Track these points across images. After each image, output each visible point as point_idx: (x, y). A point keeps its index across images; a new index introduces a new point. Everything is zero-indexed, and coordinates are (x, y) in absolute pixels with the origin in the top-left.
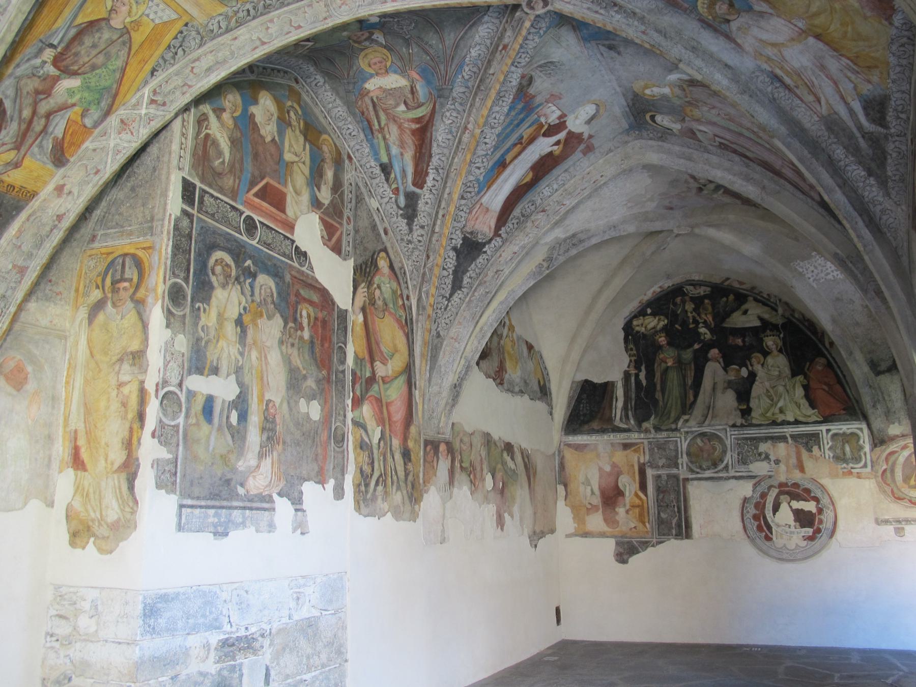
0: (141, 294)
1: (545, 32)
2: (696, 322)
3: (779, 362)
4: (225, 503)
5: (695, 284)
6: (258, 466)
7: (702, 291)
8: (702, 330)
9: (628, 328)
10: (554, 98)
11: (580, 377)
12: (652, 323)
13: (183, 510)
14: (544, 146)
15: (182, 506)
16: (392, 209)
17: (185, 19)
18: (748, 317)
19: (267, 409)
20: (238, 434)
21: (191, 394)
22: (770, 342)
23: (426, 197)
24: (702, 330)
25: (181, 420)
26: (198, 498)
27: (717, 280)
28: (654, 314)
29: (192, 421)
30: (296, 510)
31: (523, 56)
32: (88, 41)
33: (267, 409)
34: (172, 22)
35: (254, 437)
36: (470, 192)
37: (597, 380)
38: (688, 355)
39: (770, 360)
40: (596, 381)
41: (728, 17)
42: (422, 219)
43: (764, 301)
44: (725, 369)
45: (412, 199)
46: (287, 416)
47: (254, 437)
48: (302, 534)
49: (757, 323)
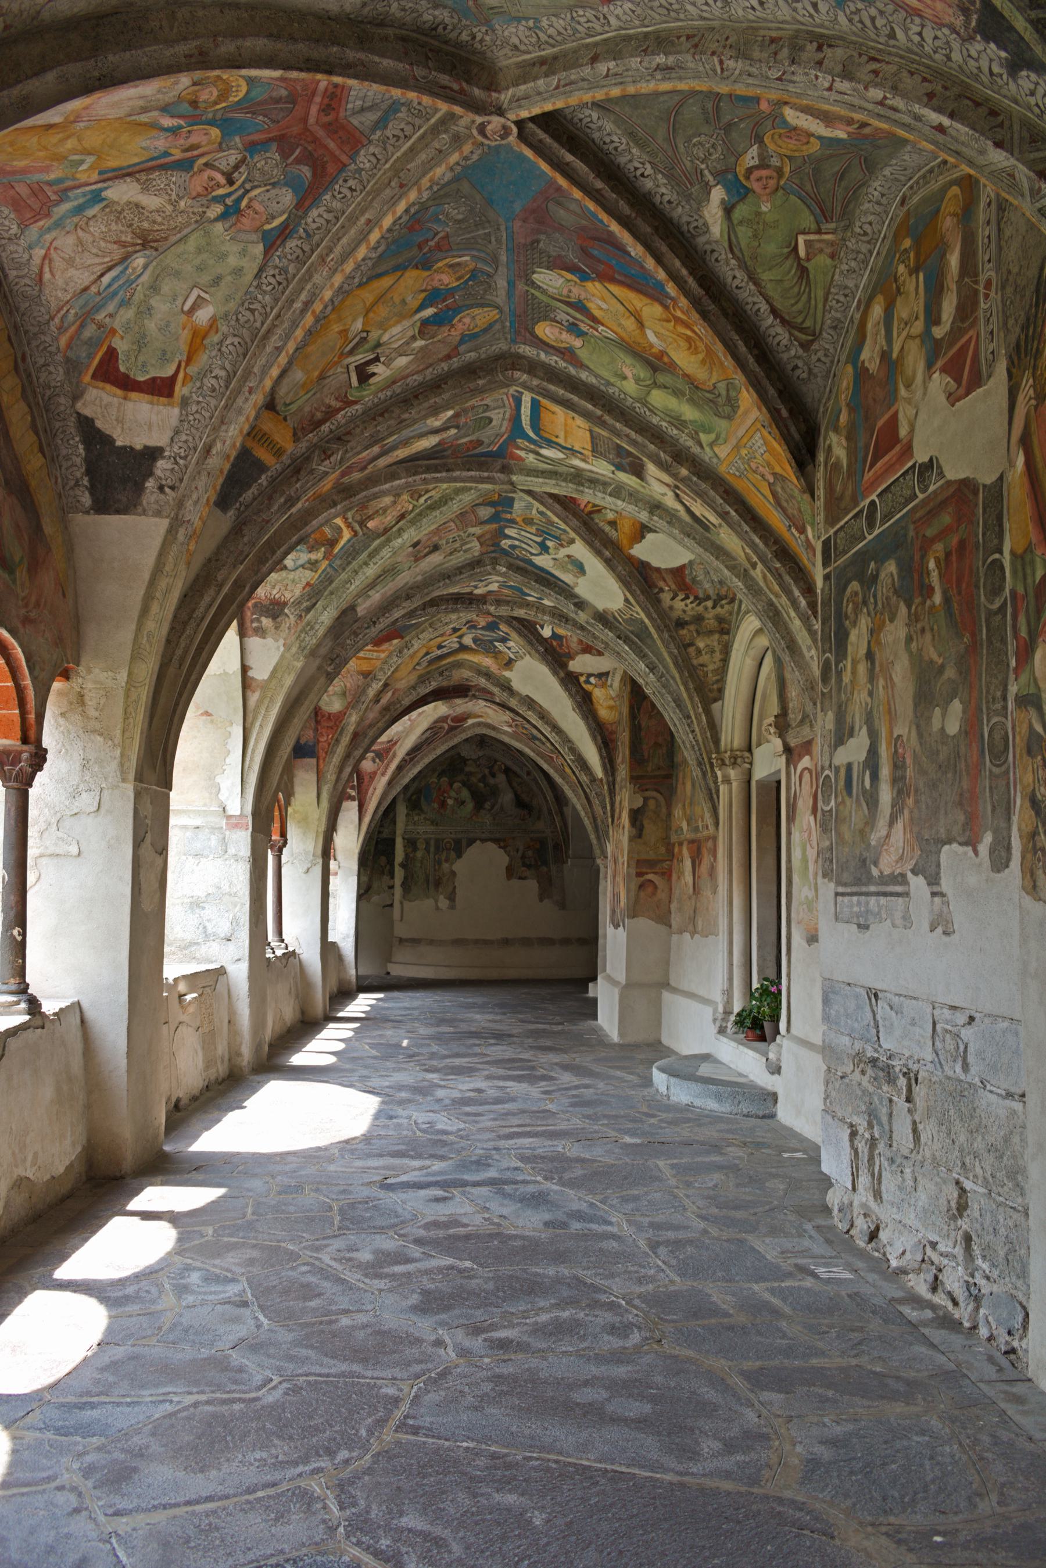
1: (527, 19)
4: (864, 889)
6: (888, 836)
13: (840, 899)
15: (837, 894)
17: (759, 426)
19: (896, 751)
20: (872, 800)
21: (837, 770)
25: (833, 803)
26: (845, 885)
29: (840, 799)
30: (934, 894)
31: (582, 20)
32: (785, 504)
33: (896, 751)
34: (763, 438)
35: (886, 795)
36: (873, 19)
41: (196, 88)
46: (918, 748)
47: (886, 795)
48: (945, 933)
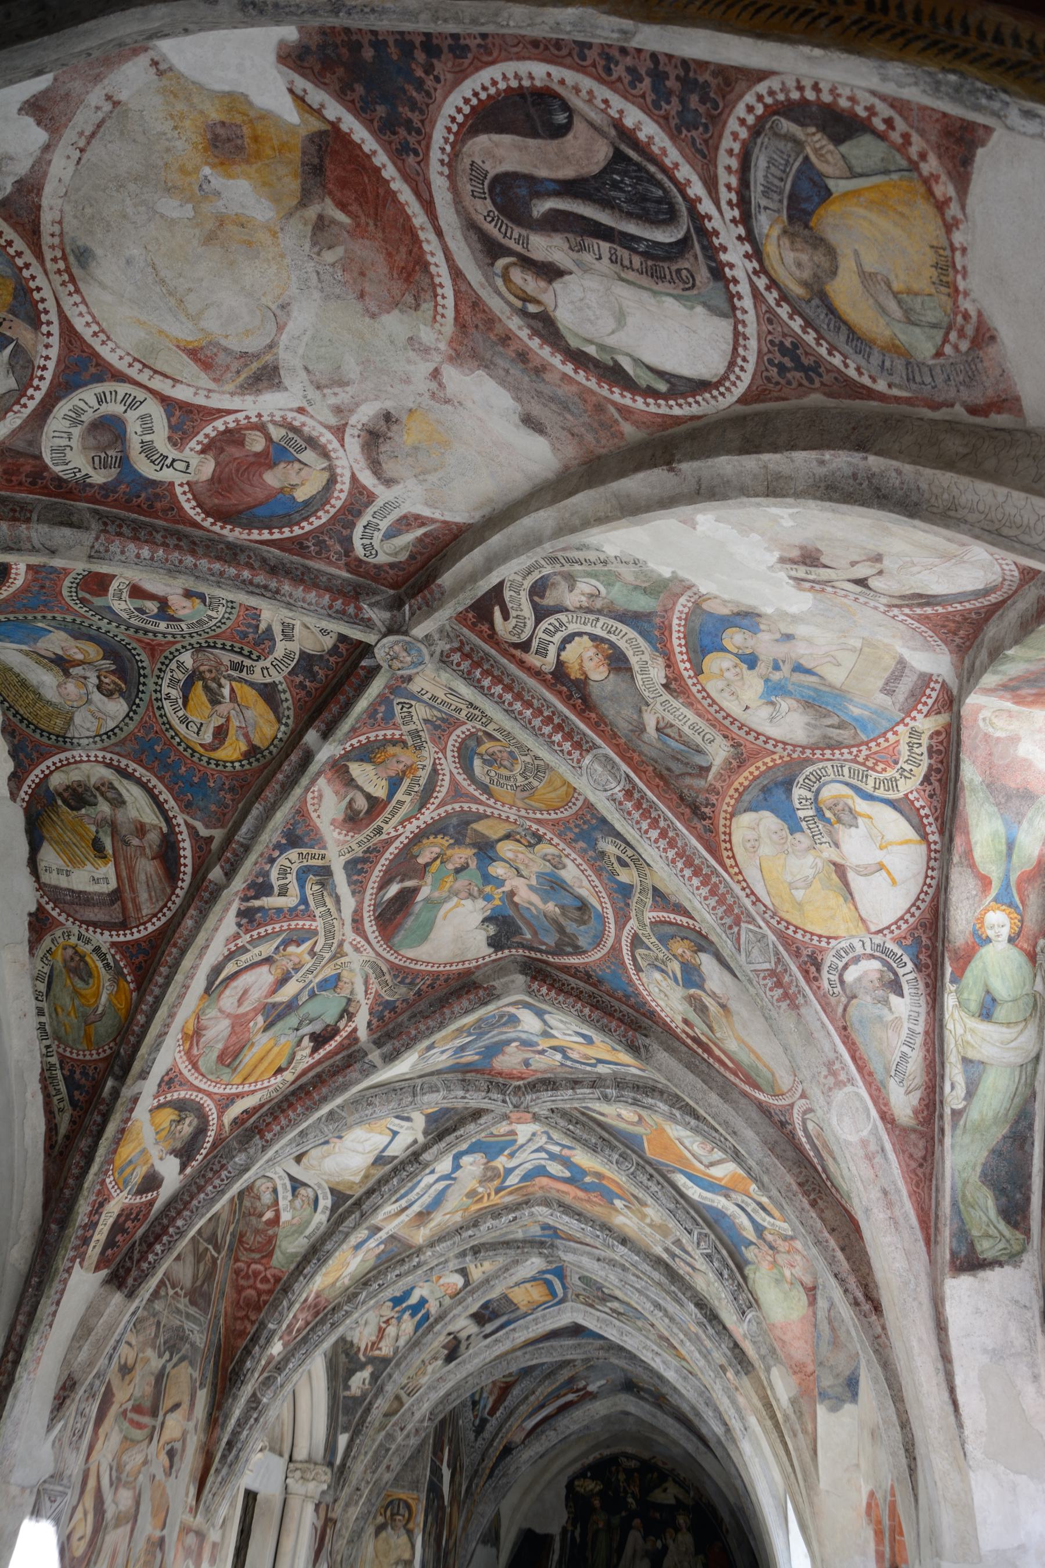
0: (411, 1526)
2: (626, 1492)
3: (686, 1539)
5: (629, 1457)
7: (633, 1464)
8: (630, 1500)
9: (570, 1486)
10: (585, 1378)
11: (526, 1525)
12: (590, 1486)
14: (571, 1397)
16: (469, 1426)
18: (667, 1495)
22: (681, 1520)
23: (493, 1423)
24: (630, 1500)
27: (646, 1455)
28: (592, 1478)
37: (538, 1530)
38: (616, 1521)
39: (680, 1536)
40: (538, 1530)
42: (486, 1434)
43: (680, 1483)
44: (645, 1538)
45: (484, 1422)
49: (672, 1501)
